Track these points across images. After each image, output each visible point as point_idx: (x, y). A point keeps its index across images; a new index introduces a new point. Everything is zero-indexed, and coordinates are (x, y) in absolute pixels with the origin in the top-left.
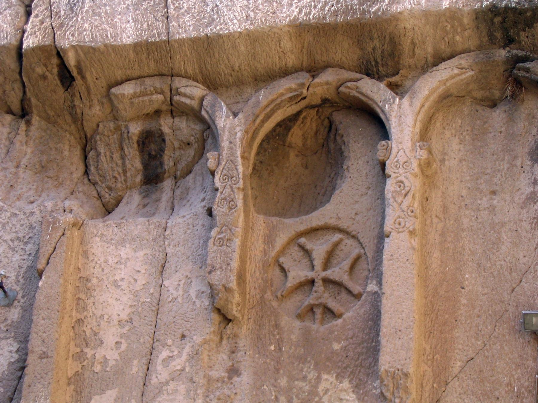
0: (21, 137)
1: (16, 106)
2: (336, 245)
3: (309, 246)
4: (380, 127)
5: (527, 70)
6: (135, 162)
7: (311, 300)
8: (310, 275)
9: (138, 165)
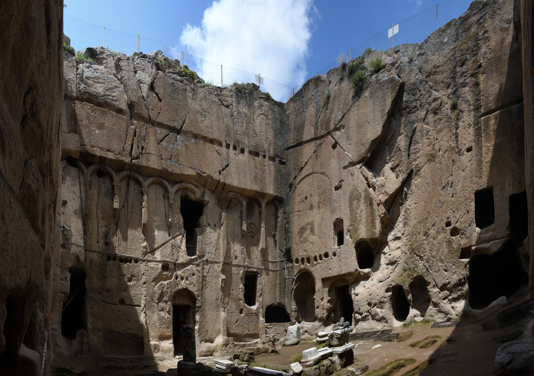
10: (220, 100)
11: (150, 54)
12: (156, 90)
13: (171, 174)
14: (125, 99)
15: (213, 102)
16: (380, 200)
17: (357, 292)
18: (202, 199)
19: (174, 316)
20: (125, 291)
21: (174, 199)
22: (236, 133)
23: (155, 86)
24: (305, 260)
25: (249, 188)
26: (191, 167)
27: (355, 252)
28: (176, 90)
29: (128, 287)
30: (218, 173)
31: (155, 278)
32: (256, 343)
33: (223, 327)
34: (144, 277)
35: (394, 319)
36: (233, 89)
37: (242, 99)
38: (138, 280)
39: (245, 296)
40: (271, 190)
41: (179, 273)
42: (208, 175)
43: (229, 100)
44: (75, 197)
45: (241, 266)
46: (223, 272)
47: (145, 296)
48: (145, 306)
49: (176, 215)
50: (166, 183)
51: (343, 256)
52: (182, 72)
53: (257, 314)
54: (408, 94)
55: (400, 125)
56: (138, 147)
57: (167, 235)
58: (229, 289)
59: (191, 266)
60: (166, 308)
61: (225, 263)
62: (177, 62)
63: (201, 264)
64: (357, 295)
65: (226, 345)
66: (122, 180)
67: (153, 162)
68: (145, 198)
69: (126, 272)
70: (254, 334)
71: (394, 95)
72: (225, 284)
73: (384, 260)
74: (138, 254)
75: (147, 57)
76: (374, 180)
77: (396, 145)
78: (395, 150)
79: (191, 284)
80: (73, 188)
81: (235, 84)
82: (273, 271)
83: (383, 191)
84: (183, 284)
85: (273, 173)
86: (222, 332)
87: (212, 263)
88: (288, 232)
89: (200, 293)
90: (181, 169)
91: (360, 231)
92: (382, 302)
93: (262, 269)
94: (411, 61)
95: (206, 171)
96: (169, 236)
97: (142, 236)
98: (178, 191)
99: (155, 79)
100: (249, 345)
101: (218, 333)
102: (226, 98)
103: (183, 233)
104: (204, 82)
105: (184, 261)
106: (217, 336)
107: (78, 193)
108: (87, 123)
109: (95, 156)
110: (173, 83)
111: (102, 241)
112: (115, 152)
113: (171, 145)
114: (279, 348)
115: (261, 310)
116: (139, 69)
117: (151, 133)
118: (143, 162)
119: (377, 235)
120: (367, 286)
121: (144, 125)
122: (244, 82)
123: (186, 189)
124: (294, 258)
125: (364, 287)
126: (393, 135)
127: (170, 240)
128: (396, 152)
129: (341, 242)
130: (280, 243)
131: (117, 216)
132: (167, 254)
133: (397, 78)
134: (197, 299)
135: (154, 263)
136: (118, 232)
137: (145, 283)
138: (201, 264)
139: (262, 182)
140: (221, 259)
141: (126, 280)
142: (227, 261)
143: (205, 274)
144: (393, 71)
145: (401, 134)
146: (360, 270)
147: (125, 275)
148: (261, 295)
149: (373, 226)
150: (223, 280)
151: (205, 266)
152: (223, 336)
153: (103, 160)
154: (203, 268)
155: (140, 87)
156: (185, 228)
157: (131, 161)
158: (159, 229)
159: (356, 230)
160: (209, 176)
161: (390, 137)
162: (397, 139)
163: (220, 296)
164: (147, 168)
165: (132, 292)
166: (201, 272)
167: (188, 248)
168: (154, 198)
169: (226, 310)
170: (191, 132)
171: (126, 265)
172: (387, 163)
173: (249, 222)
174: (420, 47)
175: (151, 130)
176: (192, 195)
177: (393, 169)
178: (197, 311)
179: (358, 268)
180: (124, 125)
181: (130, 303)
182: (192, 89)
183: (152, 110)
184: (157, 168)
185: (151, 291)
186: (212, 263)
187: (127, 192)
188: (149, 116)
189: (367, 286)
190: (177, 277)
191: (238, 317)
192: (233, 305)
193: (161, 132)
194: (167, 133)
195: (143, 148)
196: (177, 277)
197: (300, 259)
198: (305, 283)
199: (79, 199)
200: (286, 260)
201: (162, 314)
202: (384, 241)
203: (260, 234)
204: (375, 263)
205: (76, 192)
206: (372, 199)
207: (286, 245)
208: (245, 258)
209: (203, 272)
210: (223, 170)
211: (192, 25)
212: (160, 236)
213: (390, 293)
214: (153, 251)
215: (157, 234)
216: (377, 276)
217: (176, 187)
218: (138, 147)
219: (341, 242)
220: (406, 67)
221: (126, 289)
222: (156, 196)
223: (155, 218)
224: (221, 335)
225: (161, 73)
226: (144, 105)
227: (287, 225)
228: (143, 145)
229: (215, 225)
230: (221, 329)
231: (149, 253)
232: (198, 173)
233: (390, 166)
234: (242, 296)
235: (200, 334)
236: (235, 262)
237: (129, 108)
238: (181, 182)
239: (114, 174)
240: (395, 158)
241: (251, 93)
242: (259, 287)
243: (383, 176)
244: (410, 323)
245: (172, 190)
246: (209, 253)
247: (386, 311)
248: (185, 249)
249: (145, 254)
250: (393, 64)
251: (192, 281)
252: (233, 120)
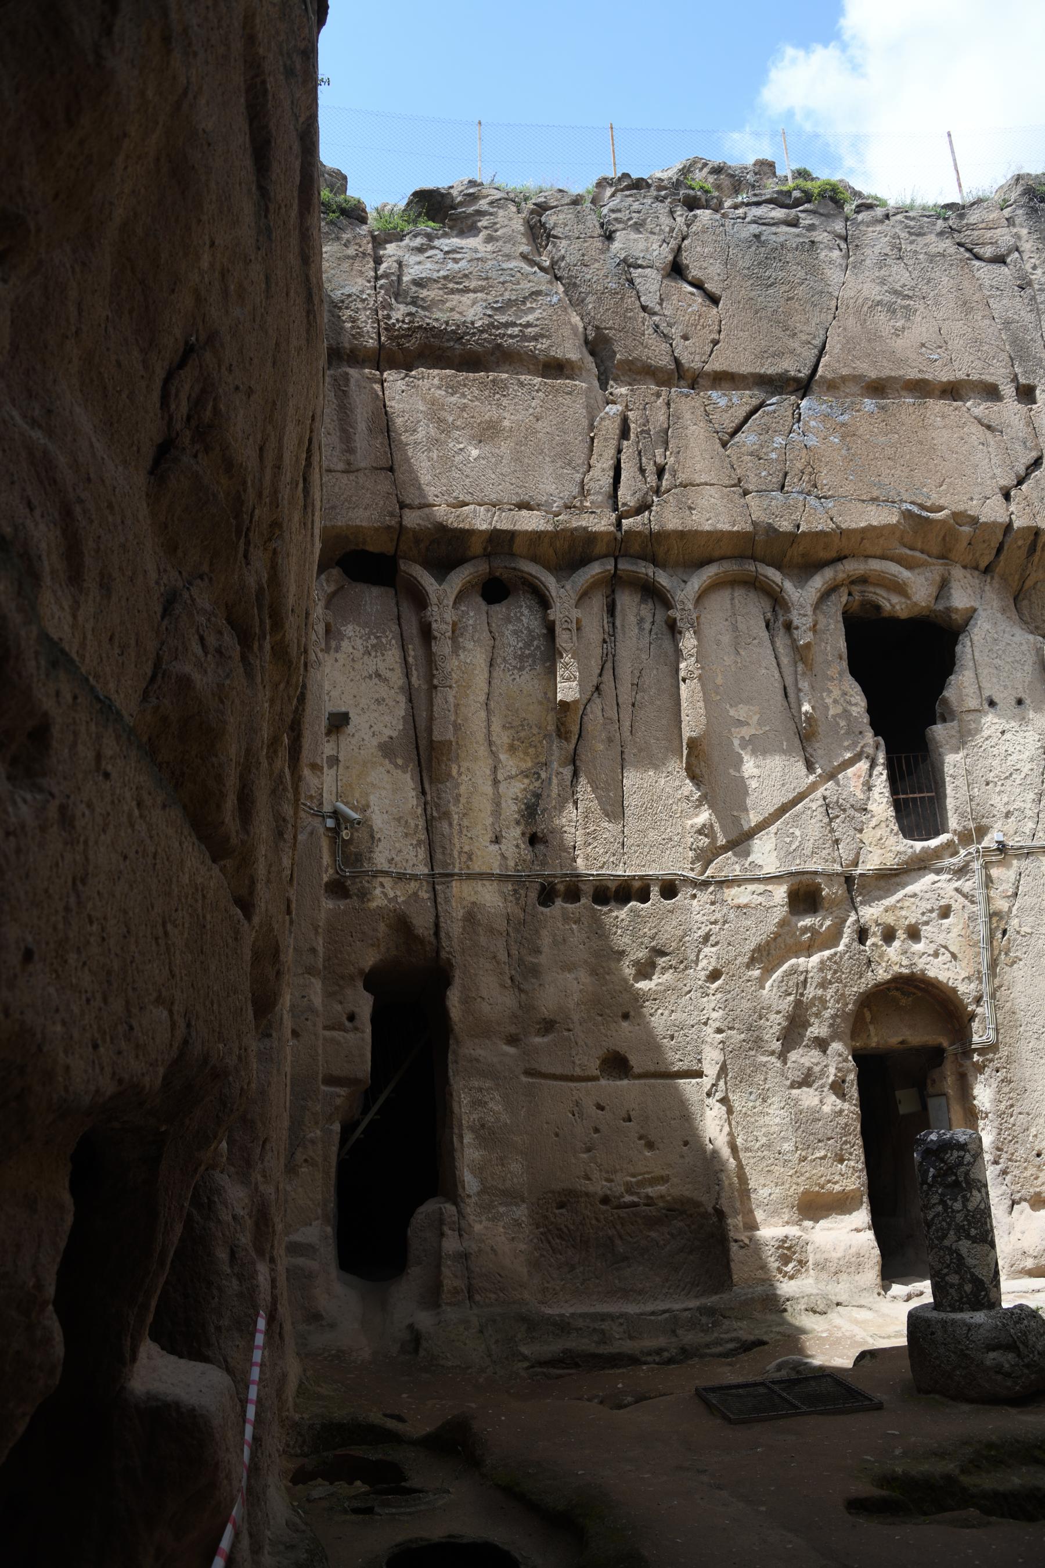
0: (987, 588)
1: (983, 565)
10: (960, 244)
11: (659, 175)
12: (694, 273)
13: (793, 538)
14: (574, 328)
15: (932, 258)
18: (940, 607)
19: (865, 1103)
20: (626, 1016)
21: (814, 628)
23: (686, 259)
26: (874, 500)
28: (776, 254)
29: (638, 999)
30: (1000, 497)
31: (758, 949)
34: (707, 950)
36: (1013, 196)
38: (683, 965)
41: (871, 913)
42: (955, 515)
43: (1004, 237)
44: (383, 691)
47: (719, 1031)
48: (723, 1070)
49: (830, 685)
50: (774, 575)
52: (789, 193)
56: (642, 471)
57: (800, 767)
59: (931, 877)
60: (823, 1073)
62: (766, 167)
63: (976, 865)
66: (584, 596)
67: (712, 512)
68: (688, 642)
69: (626, 940)
74: (675, 863)
75: (649, 186)
79: (936, 955)
80: (372, 664)
84: (894, 959)
87: (1028, 853)
89: (986, 989)
90: (833, 512)
95: (942, 502)
96: (810, 767)
97: (689, 786)
98: (826, 595)
99: (683, 239)
102: (989, 234)
103: (870, 750)
104: (883, 204)
105: (891, 862)
107: (397, 678)
108: (433, 431)
109: (470, 533)
110: (757, 236)
111: (514, 834)
112: (549, 504)
113: (779, 440)
116: (620, 226)
117: (688, 416)
118: (667, 517)
121: (658, 395)
123: (864, 580)
127: (813, 787)
131: (575, 729)
132: (810, 844)
134: (972, 1016)
135: (751, 887)
136: (584, 787)
137: (714, 975)
138: (976, 865)
141: (629, 971)
143: (1002, 905)
147: (622, 953)
151: (995, 872)
153: (500, 541)
155: (631, 281)
156: (878, 728)
157: (619, 525)
158: (760, 747)
164: (682, 535)
165: (660, 1020)
166: (979, 897)
167: (900, 807)
168: (726, 639)
170: (856, 379)
171: (623, 913)
175: (688, 405)
176: (895, 599)
178: (980, 1069)
180: (576, 408)
181: (652, 1068)
182: (840, 237)
183: (686, 338)
184: (727, 527)
185: (746, 1005)
186: (1028, 853)
187: (611, 636)
188: (677, 361)
190: (862, 935)
193: (730, 404)
194: (755, 402)
195: (660, 472)
196: (862, 935)
199: (402, 699)
201: (808, 1098)
205: (388, 674)
209: (988, 899)
210: (1020, 482)
211: (804, 44)
212: (767, 777)
214: (740, 841)
215: (756, 772)
217: (818, 582)
218: (642, 471)
221: (631, 1009)
222: (735, 629)
223: (740, 712)
225: (704, 215)
226: (651, 330)
228: (660, 460)
229: (1020, 702)
231: (725, 849)
232: (907, 515)
235: (1004, 1172)
237: (592, 353)
238: (840, 559)
239: (550, 582)
245: (802, 595)
246: (1008, 815)
248: (891, 812)
249: (706, 856)
251: (941, 939)
252: (1033, 298)
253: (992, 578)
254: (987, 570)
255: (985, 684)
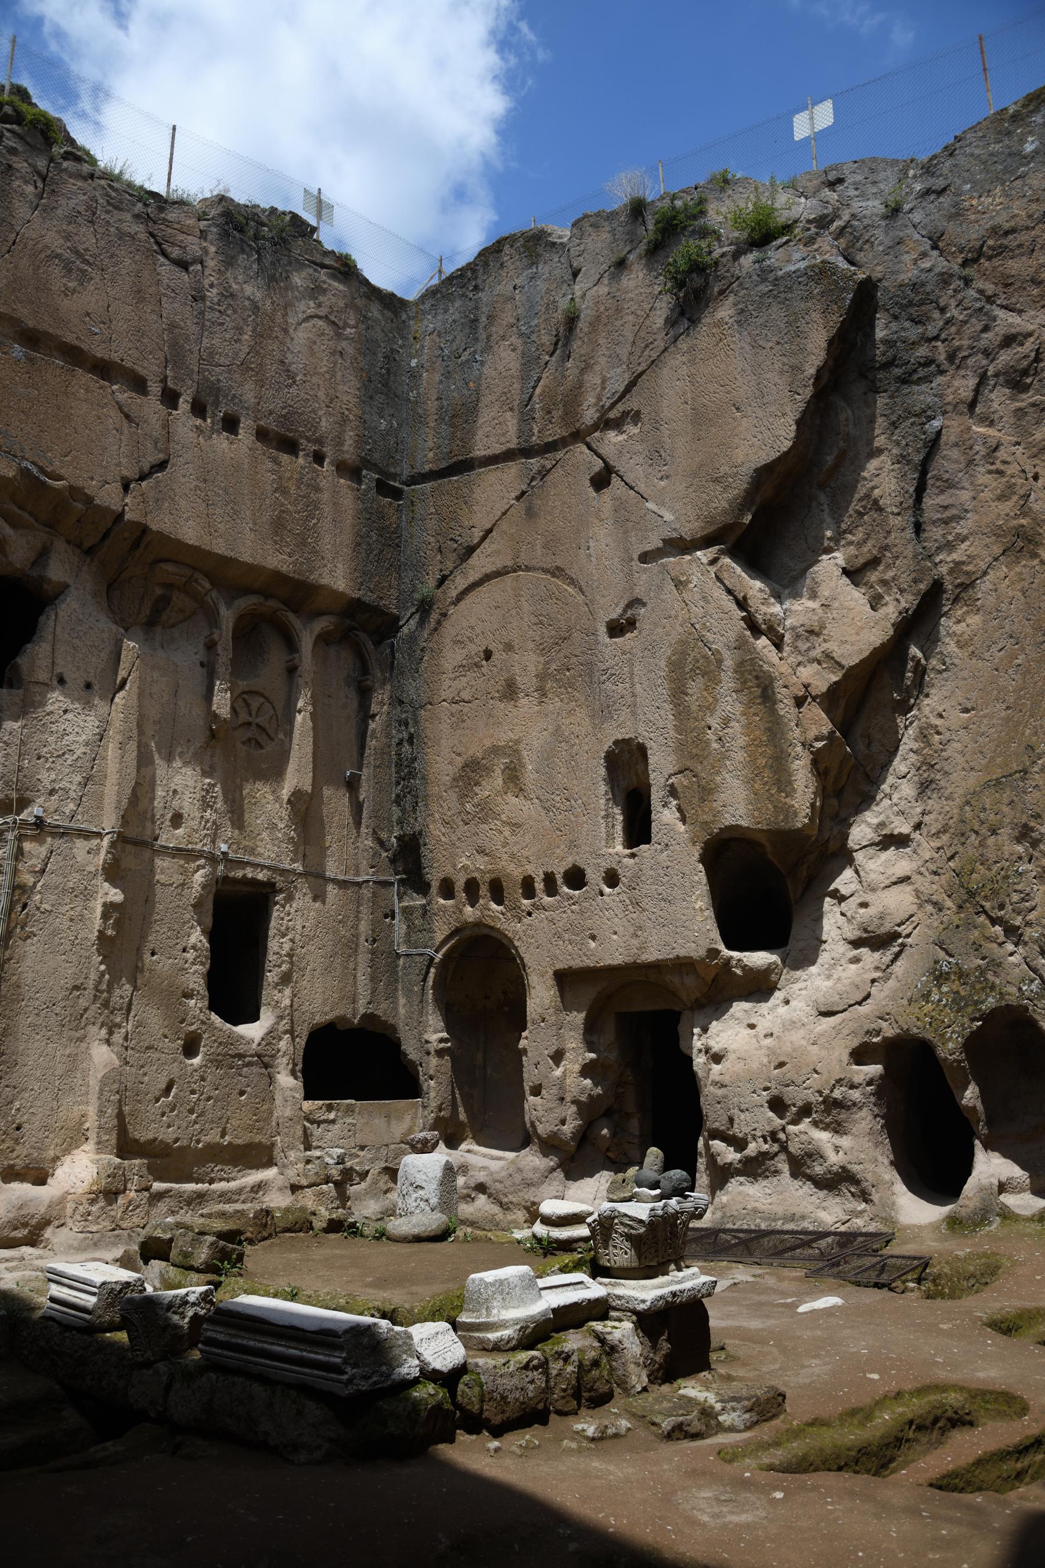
0: (85, 568)
1: (87, 545)
2: (262, 704)
3: (250, 702)
4: (291, 644)
5: (357, 635)
6: (146, 611)
7: (249, 734)
8: (250, 719)
9: (148, 612)
10: (152, 235)
15: (122, 235)
16: (806, 686)
17: (716, 1047)
22: (209, 358)
24: (484, 890)
25: (250, 560)
27: (702, 877)
32: (259, 1187)
33: (101, 1112)
35: (900, 1187)
36: (213, 213)
37: (243, 251)
39: (212, 979)
40: (337, 576)
42: (72, 488)
43: (193, 246)
45: (200, 855)
46: (113, 873)
51: (647, 888)
53: (264, 1060)
54: (896, 318)
55: (872, 421)
58: (139, 951)
61: (121, 840)
63: (10, 836)
64: (717, 1058)
65: (109, 1193)
70: (250, 1146)
71: (836, 319)
72: (118, 925)
73: (835, 924)
76: (777, 609)
77: (861, 491)
78: (855, 506)
81: (222, 199)
82: (343, 884)
83: (817, 653)
85: (349, 519)
86: (92, 1135)
87: (64, 833)
88: (412, 775)
91: (722, 797)
92: (838, 1104)
93: (293, 872)
94: (894, 212)
95: (62, 472)
100: (225, 1197)
101: (75, 1138)
102: (181, 237)
104: (93, 161)
106: (67, 1151)
114: (367, 1212)
115: (284, 1044)
119: (801, 820)
120: (764, 1024)
122: (257, 201)
124: (434, 877)
125: (752, 1026)
126: (843, 454)
128: (861, 515)
129: (638, 831)
130: (375, 815)
133: (843, 264)
138: (10, 836)
139: (304, 543)
140: (109, 822)
142: (132, 833)
143: (28, 879)
144: (825, 242)
145: (879, 452)
146: (726, 953)
148: (286, 979)
149: (783, 781)
150: (109, 909)
151: (27, 846)
152: (99, 1151)
154: (19, 854)
159: (706, 792)
160: (75, 491)
161: (830, 459)
162: (863, 468)
163: (93, 976)
169: (118, 1037)
172: (828, 551)
173: (243, 685)
174: (928, 169)
177: (853, 574)
179: (721, 947)
182: (39, 174)
186: (64, 833)
189: (764, 1024)
191: (174, 1070)
192: (151, 1018)
197: (460, 882)
198: (481, 982)
200: (401, 882)
202: (833, 846)
203: (289, 734)
204: (798, 932)
206: (771, 679)
207: (400, 822)
208: (217, 827)
209: (15, 872)
210: (142, 478)
213: (875, 1069)
216: (808, 987)
219: (638, 831)
220: (879, 233)
224: (89, 1146)
227: (406, 748)
229: (88, 686)
230: (91, 1123)
232: (25, 473)
233: (841, 562)
234: (195, 978)
236: (170, 837)
240: (859, 535)
241: (281, 242)
242: (277, 946)
243: (813, 596)
244: (982, 1217)
246: (52, 792)
247: (859, 1145)
250: (822, 222)
252: (202, 313)
253: (92, 560)
254: (89, 552)
255: (59, 661)
